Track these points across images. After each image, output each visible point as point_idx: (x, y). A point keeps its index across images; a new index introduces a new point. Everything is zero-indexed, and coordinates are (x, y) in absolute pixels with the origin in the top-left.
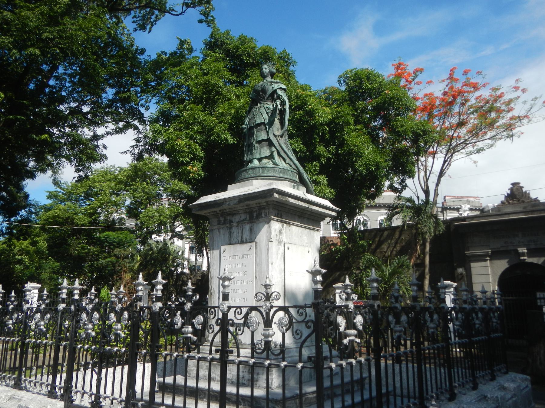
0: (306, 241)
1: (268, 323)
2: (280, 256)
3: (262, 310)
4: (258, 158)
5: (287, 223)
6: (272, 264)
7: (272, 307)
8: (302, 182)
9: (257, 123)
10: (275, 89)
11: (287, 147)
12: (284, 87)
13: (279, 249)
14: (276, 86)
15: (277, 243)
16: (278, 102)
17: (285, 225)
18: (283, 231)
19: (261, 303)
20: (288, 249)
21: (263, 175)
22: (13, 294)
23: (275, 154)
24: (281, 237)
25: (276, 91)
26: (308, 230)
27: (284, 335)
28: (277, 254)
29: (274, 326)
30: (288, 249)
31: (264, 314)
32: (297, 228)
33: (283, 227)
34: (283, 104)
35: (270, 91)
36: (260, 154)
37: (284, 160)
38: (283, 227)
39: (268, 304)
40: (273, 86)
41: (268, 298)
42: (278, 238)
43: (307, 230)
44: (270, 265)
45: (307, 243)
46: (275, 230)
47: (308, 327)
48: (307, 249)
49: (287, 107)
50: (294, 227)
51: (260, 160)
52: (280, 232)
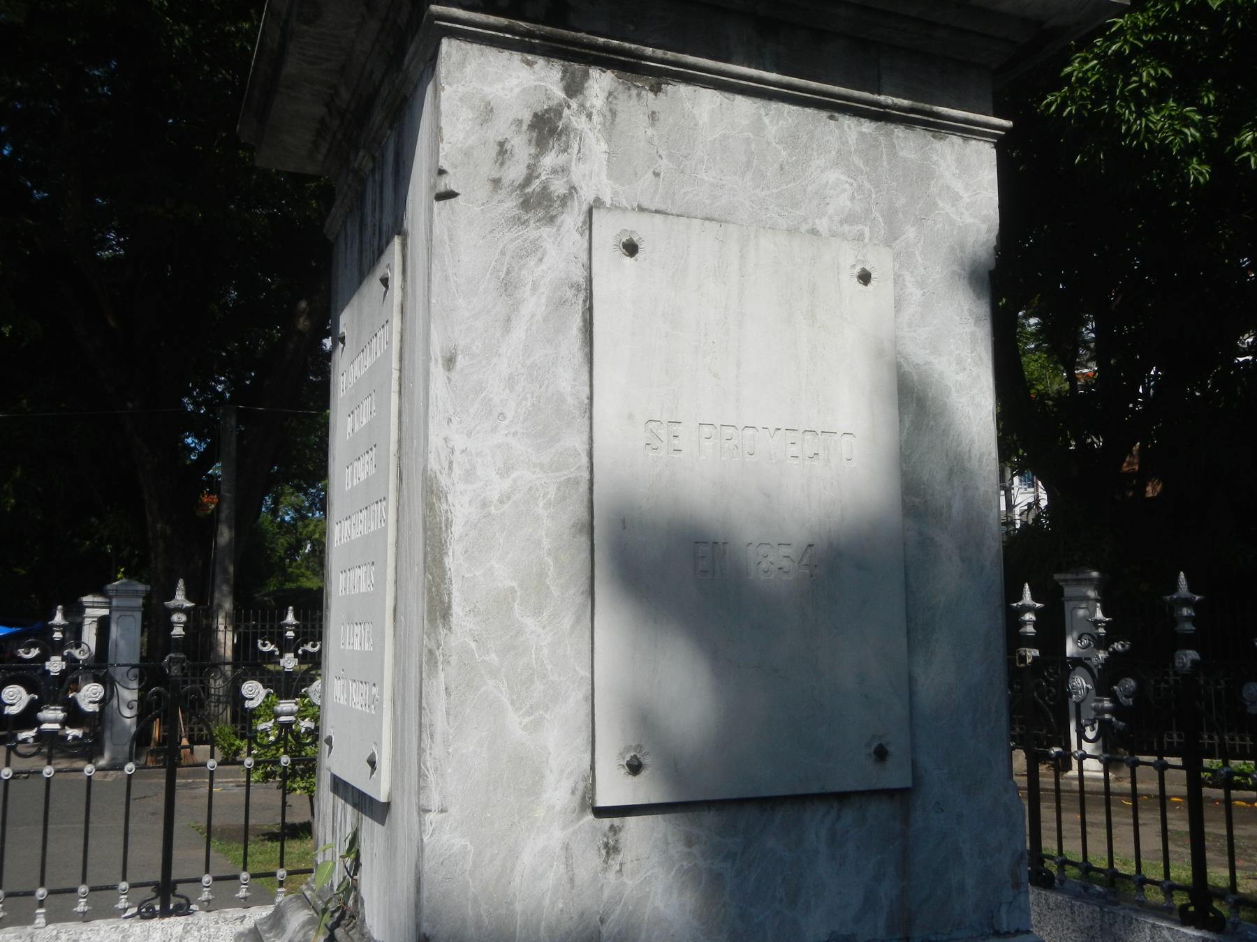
0: (843, 201)
2: (534, 305)
5: (627, 67)
6: (450, 362)
13: (534, 248)
15: (510, 205)
17: (600, 82)
18: (572, 118)
22: (290, 618)
24: (550, 160)
26: (868, 126)
28: (508, 286)
30: (631, 249)
32: (743, 104)
33: (574, 88)
38: (574, 88)
42: (515, 172)
43: (853, 129)
44: (437, 370)
46: (487, 112)
50: (709, 99)
52: (546, 127)
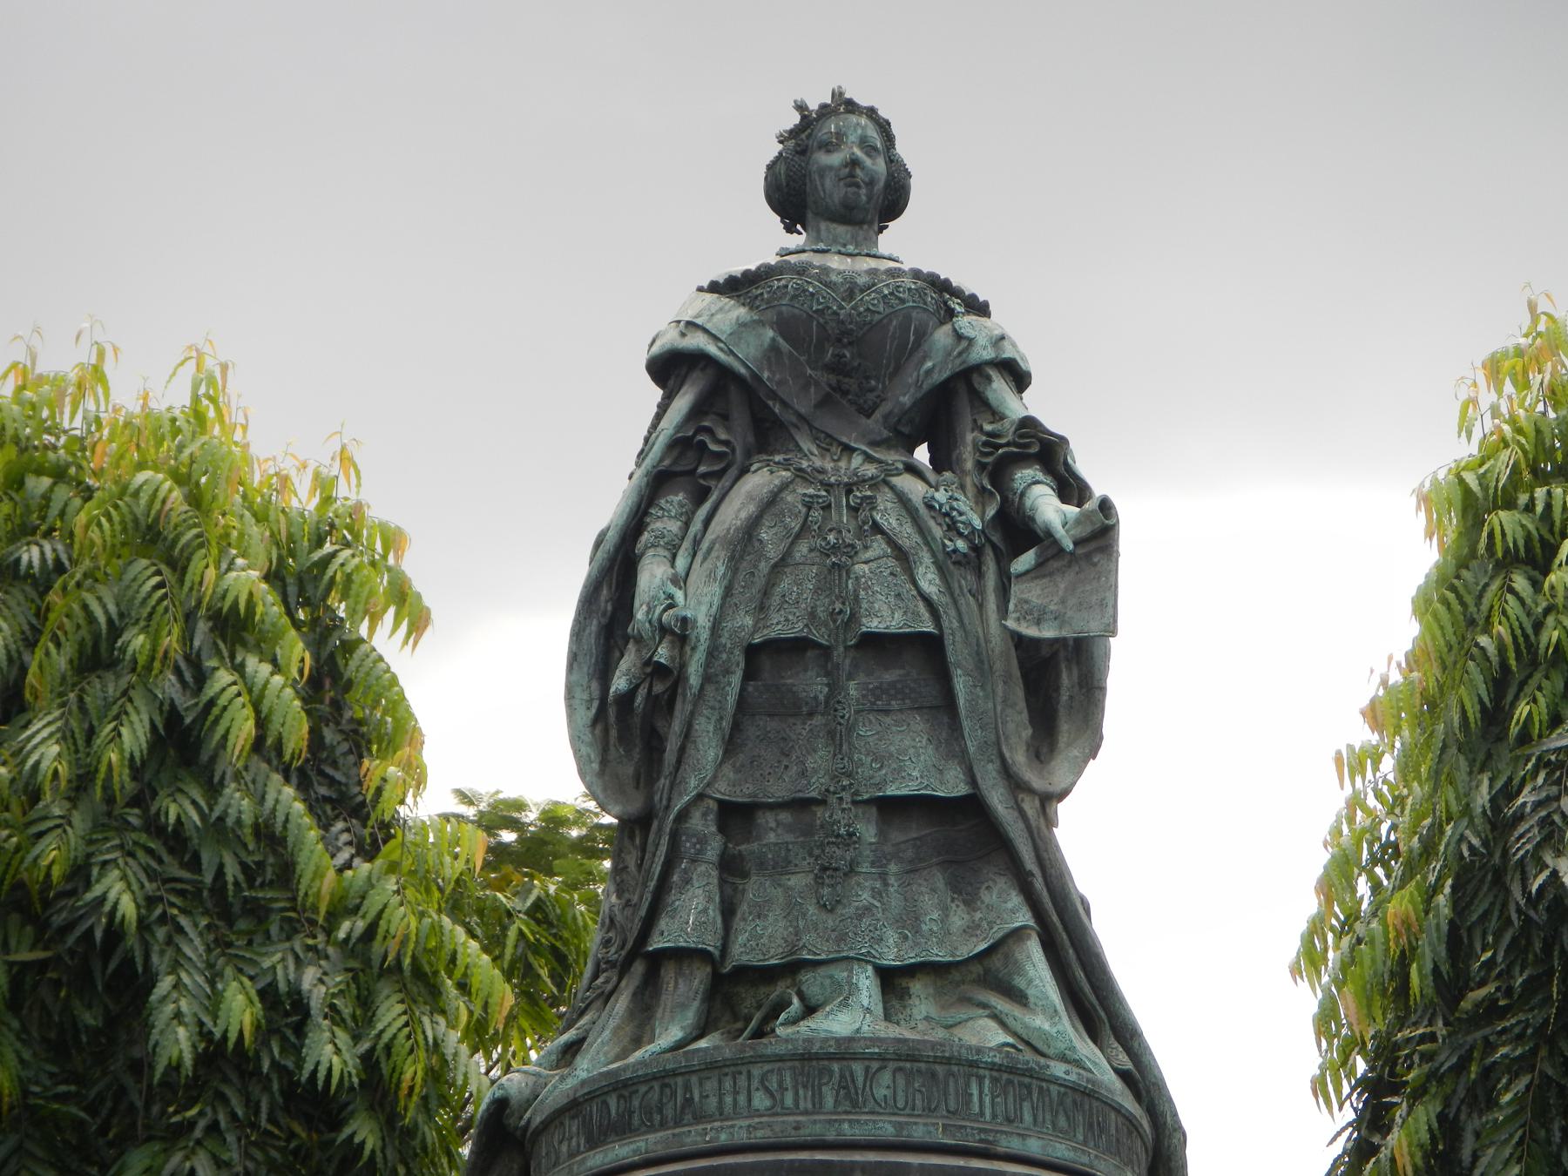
4: (890, 958)
9: (873, 625)
36: (910, 922)
51: (892, 981)
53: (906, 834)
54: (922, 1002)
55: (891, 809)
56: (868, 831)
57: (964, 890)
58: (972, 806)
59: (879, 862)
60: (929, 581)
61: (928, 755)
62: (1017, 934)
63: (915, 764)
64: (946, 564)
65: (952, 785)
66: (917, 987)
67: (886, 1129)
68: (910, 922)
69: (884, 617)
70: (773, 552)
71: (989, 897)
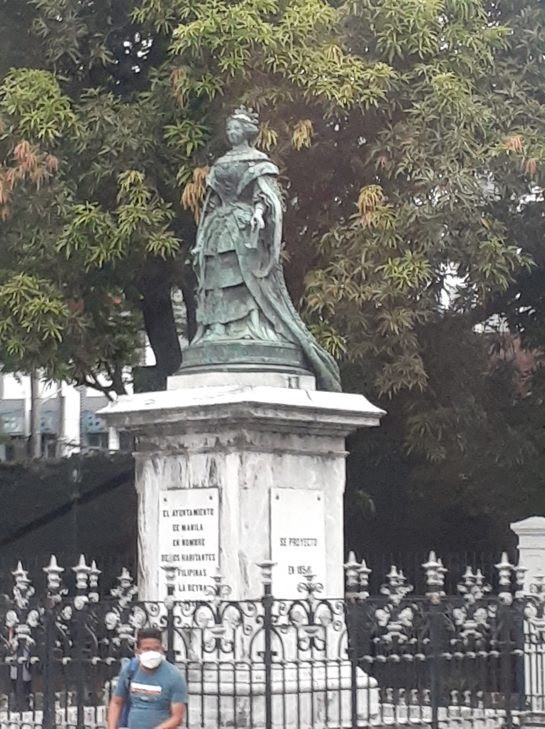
1: (218, 619)
2: (261, 512)
3: (212, 605)
7: (222, 602)
8: (309, 366)
9: (220, 251)
10: (254, 176)
11: (279, 297)
12: (274, 169)
14: (255, 169)
16: (259, 212)
19: (211, 598)
20: (277, 498)
21: (231, 360)
23: (255, 316)
25: (254, 182)
27: (234, 631)
29: (225, 623)
30: (277, 498)
31: (215, 609)
34: (268, 213)
35: (245, 181)
37: (272, 326)
39: (218, 599)
40: (251, 170)
41: (218, 592)
45: (315, 483)
47: (258, 622)
48: (317, 493)
49: (278, 218)
51: (226, 325)
53: (228, 293)
54: (233, 328)
55: (225, 289)
56: (221, 294)
57: (244, 302)
58: (243, 284)
59: (222, 300)
60: (236, 235)
61: (232, 275)
62: (253, 310)
63: (229, 279)
64: (241, 230)
65: (239, 281)
66: (232, 326)
67: (207, 361)
68: (226, 313)
69: (223, 248)
70: (209, 235)
71: (248, 302)
